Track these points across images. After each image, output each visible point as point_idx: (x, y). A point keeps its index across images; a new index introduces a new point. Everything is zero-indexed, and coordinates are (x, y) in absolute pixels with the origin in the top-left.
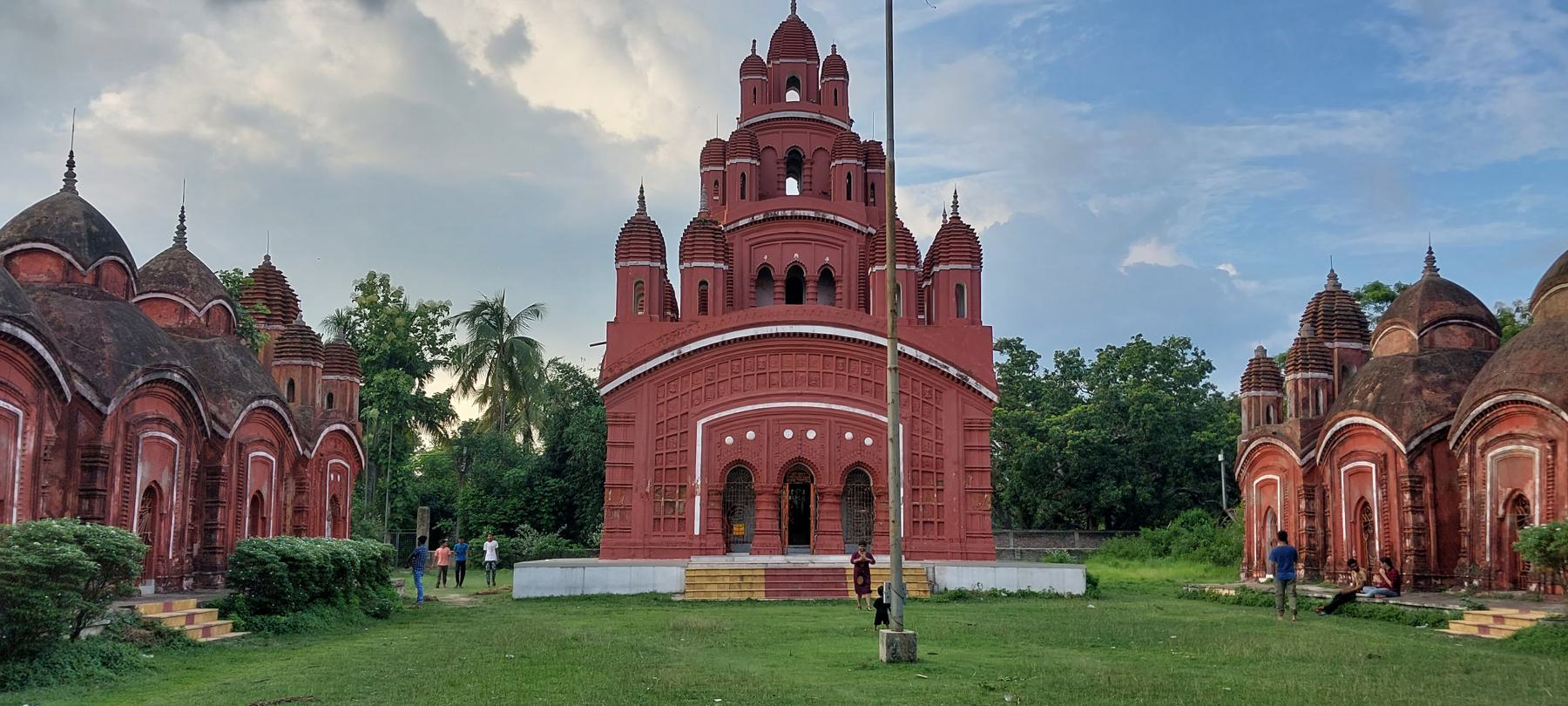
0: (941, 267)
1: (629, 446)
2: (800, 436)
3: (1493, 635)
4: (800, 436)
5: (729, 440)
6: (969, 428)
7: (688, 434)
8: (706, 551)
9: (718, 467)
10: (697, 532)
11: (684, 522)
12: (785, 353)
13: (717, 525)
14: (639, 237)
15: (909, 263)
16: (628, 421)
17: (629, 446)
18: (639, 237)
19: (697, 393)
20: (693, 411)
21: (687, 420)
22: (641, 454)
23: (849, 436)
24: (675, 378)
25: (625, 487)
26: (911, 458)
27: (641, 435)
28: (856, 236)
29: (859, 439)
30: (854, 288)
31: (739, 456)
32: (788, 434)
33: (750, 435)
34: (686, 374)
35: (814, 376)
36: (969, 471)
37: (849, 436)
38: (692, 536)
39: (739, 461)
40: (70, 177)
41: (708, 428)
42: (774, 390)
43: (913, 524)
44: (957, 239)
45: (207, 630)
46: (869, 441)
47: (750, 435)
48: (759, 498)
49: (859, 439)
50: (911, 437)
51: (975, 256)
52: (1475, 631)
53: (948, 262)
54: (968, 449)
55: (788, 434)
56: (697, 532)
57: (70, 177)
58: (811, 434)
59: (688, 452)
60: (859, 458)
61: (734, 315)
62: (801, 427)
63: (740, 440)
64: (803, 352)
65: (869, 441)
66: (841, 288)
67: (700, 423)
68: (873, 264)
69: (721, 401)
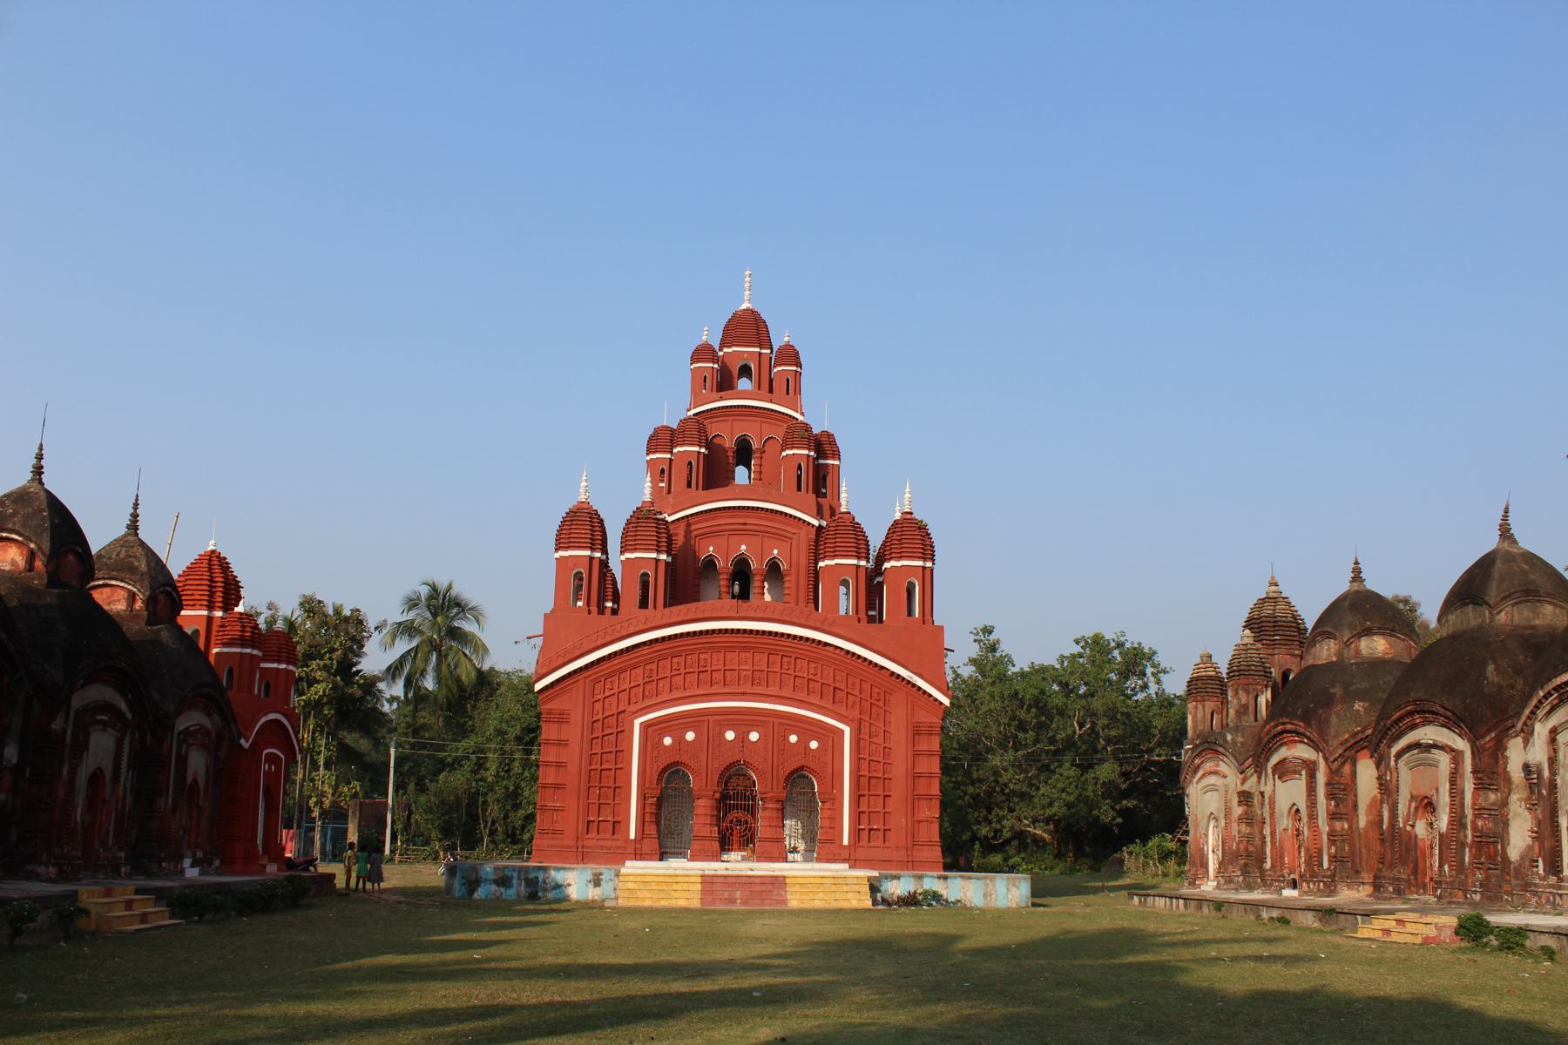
0: (894, 563)
1: (561, 743)
2: (742, 738)
3: (1394, 938)
4: (742, 738)
5: (667, 741)
6: (917, 732)
7: (624, 733)
8: (639, 856)
9: (657, 769)
10: (632, 836)
11: (618, 825)
14: (582, 525)
15: (859, 558)
16: (562, 718)
17: (561, 743)
18: (582, 525)
20: (633, 708)
22: (573, 756)
23: (793, 738)
25: (557, 787)
26: (857, 759)
27: (574, 732)
28: (807, 528)
29: (803, 743)
30: (803, 582)
32: (730, 735)
33: (690, 736)
35: (757, 674)
36: (916, 776)
37: (793, 738)
38: (627, 839)
39: (677, 763)
40: (38, 471)
41: (645, 727)
42: (715, 689)
43: (856, 833)
44: (911, 536)
45: (144, 918)
46: (814, 745)
47: (690, 736)
48: (701, 802)
49: (803, 743)
51: (927, 552)
52: (1378, 935)
53: (900, 558)
54: (917, 754)
55: (730, 735)
56: (632, 836)
57: (38, 471)
58: (754, 736)
59: (623, 753)
60: (802, 762)
61: (676, 609)
62: (744, 729)
64: (746, 649)
65: (814, 745)
66: (789, 582)
67: (637, 722)
68: (823, 559)
69: (659, 699)
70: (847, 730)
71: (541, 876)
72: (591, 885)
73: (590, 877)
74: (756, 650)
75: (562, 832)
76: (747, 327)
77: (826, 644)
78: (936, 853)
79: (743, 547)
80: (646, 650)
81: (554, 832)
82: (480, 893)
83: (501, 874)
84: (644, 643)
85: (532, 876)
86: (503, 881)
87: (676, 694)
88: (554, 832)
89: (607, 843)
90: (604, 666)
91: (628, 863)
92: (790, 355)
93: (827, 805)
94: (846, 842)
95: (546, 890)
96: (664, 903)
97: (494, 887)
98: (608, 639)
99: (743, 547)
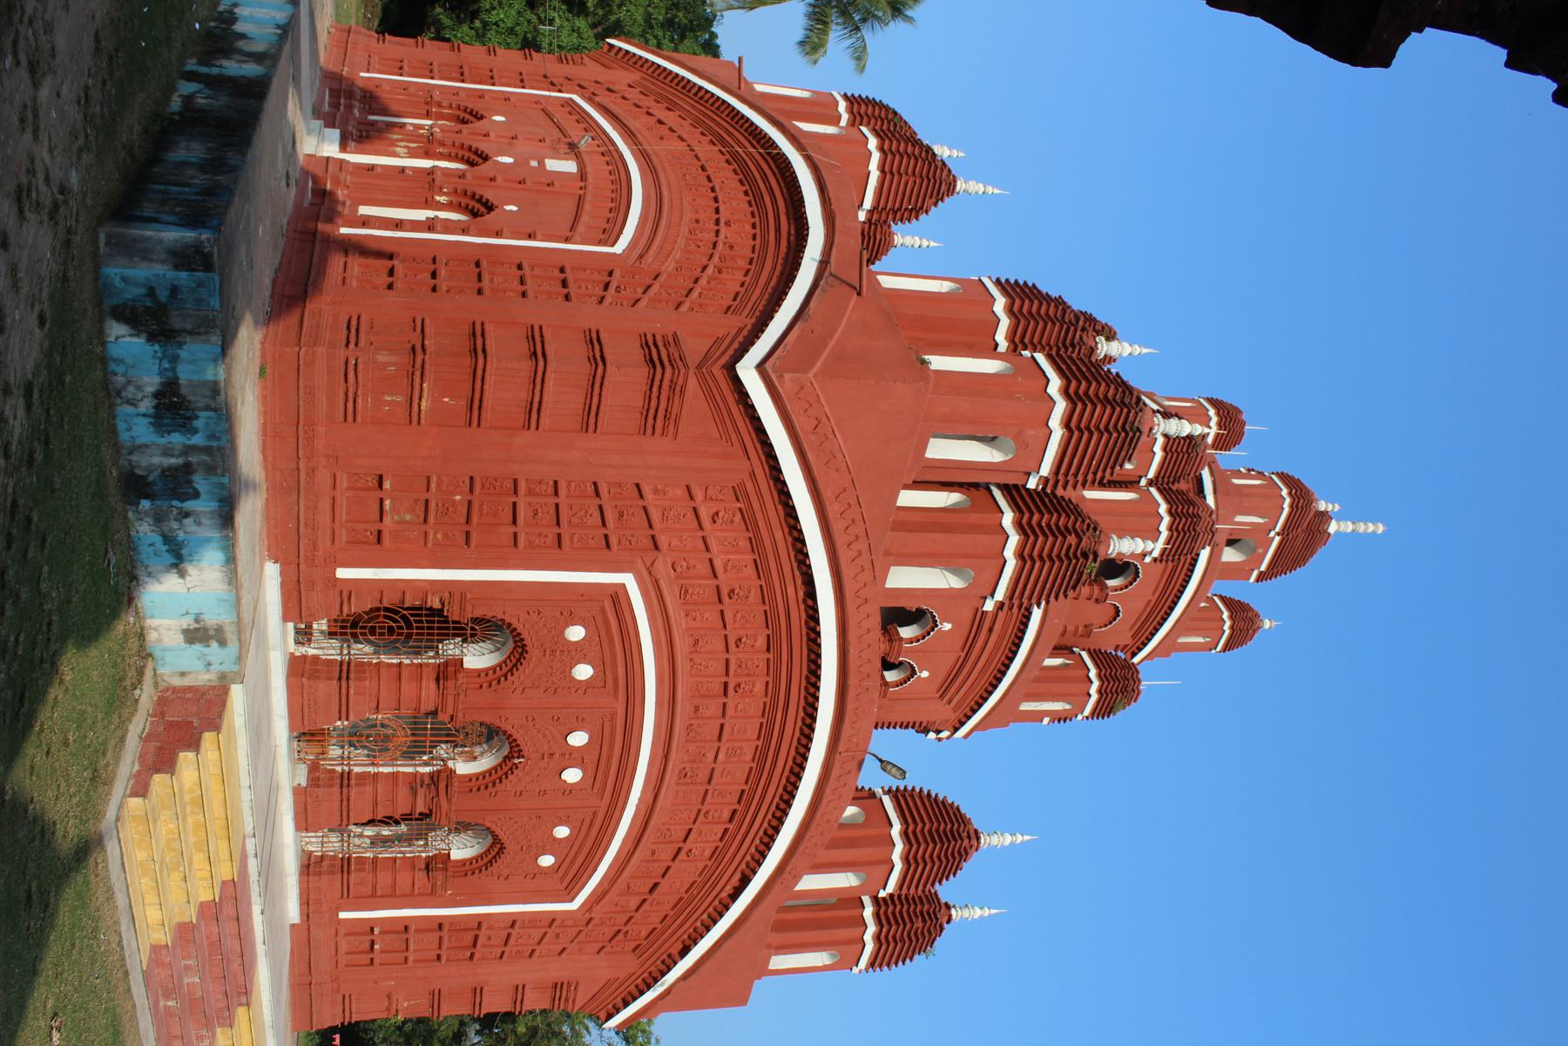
5: (576, 633)
10: (342, 573)
11: (376, 547)
12: (765, 732)
13: (357, 606)
19: (704, 569)
21: (645, 552)
24: (749, 521)
28: (953, 717)
31: (534, 653)
34: (755, 544)
37: (562, 832)
50: (552, 919)
56: (342, 573)
62: (591, 759)
63: (578, 653)
64: (760, 756)
65: (547, 861)
67: (628, 580)
70: (575, 905)
71: (204, 505)
72: (188, 622)
73: (211, 619)
74: (753, 776)
75: (351, 414)
76: (1304, 536)
77: (745, 881)
78: (330, 1017)
79: (947, 626)
80: (795, 592)
81: (351, 400)
82: (124, 342)
83: (198, 400)
84: (811, 593)
85: (200, 482)
86: (173, 406)
87: (682, 647)
88: (351, 400)
89: (324, 518)
90: (774, 512)
91: (272, 571)
92: (1245, 621)
93: (421, 876)
94: (343, 915)
95: (159, 518)
96: (142, 883)
97: (152, 382)
98: (837, 527)
99: (947, 626)
